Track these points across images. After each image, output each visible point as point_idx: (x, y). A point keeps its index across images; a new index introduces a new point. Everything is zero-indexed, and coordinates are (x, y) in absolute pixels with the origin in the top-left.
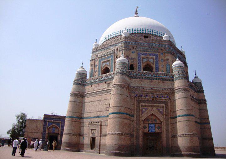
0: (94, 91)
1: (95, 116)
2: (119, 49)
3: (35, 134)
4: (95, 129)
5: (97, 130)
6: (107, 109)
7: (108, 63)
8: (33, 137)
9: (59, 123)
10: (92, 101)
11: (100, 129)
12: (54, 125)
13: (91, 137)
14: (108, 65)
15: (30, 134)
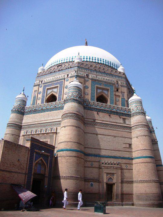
0: (103, 121)
1: (110, 155)
2: (119, 82)
3: (16, 175)
4: (112, 172)
5: (115, 175)
6: (127, 150)
7: (106, 92)
8: (12, 182)
9: (47, 156)
10: (102, 134)
11: (120, 173)
12: (41, 159)
13: (107, 184)
14: (105, 94)
15: (8, 175)
